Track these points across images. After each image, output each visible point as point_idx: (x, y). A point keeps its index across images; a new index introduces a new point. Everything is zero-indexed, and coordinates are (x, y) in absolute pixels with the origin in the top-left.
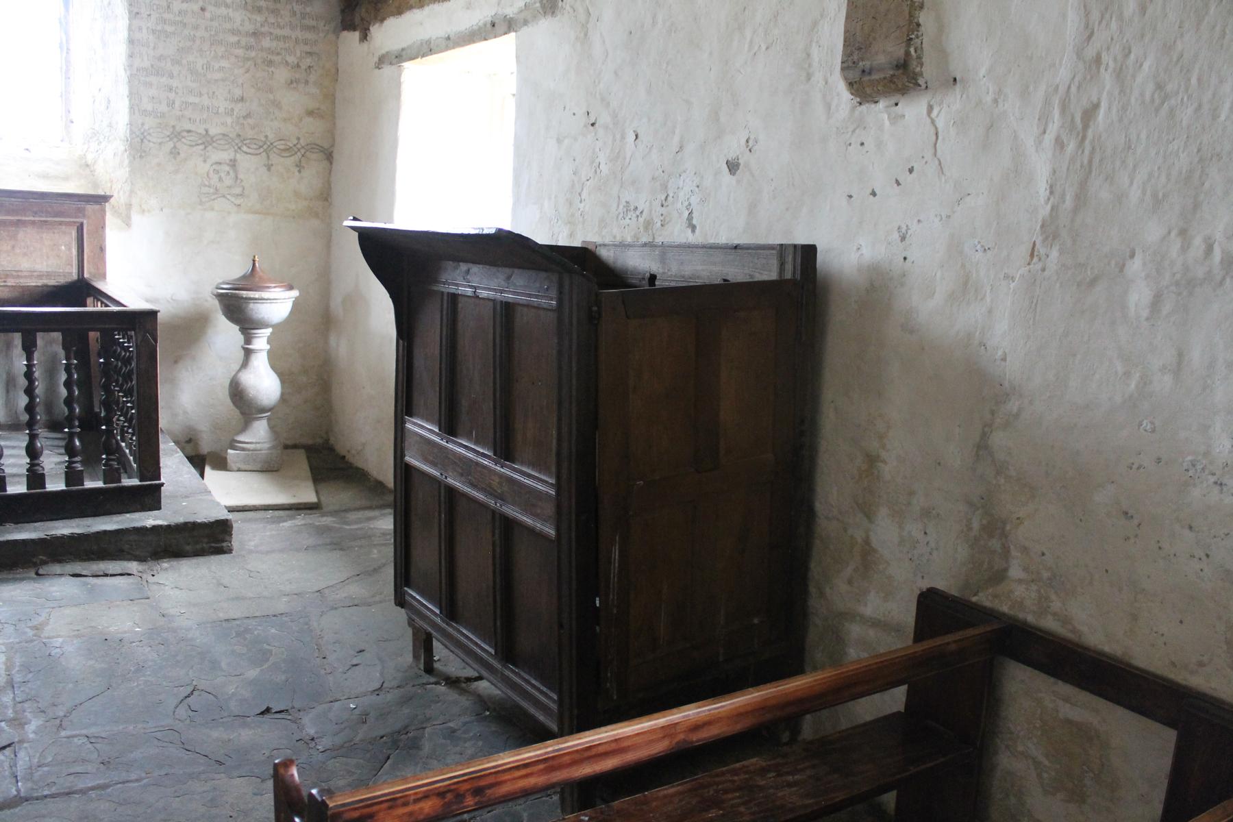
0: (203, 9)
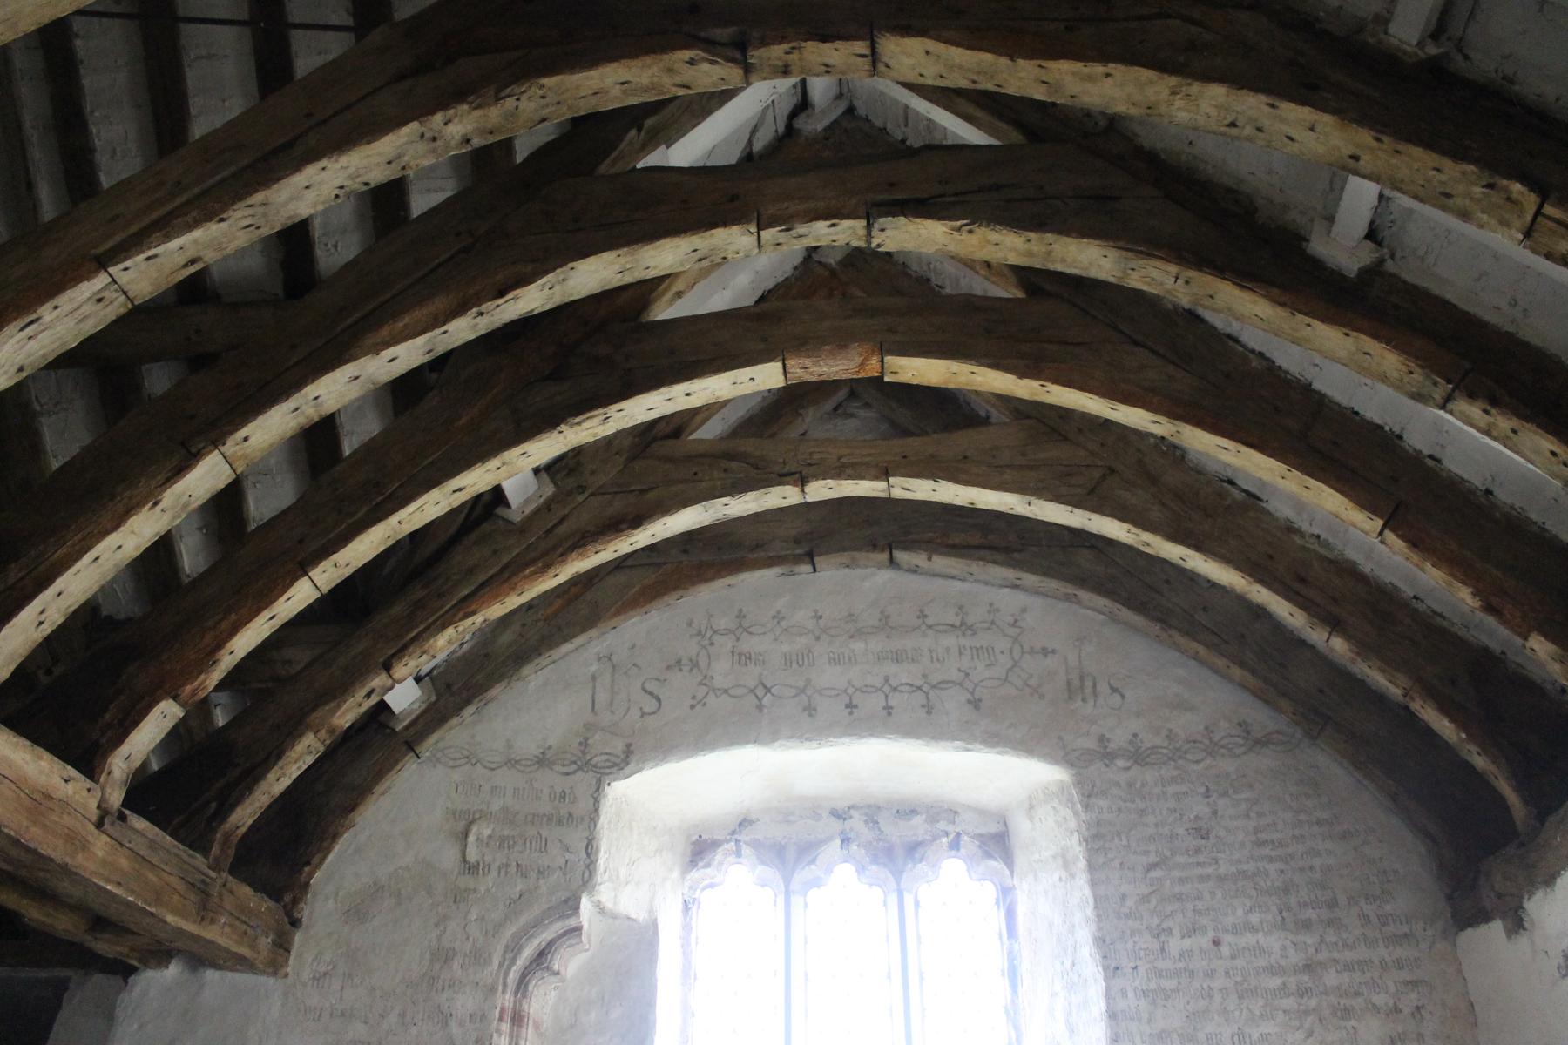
0: (1216, 943)
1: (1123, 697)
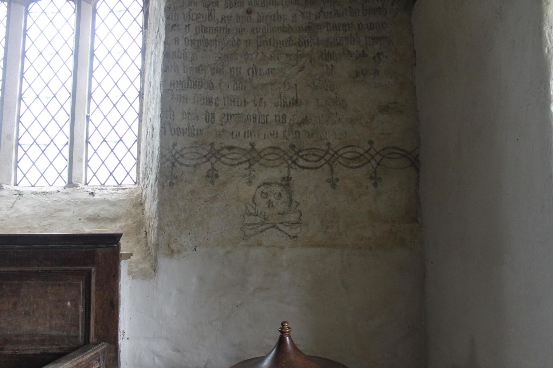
0: (249, 12)
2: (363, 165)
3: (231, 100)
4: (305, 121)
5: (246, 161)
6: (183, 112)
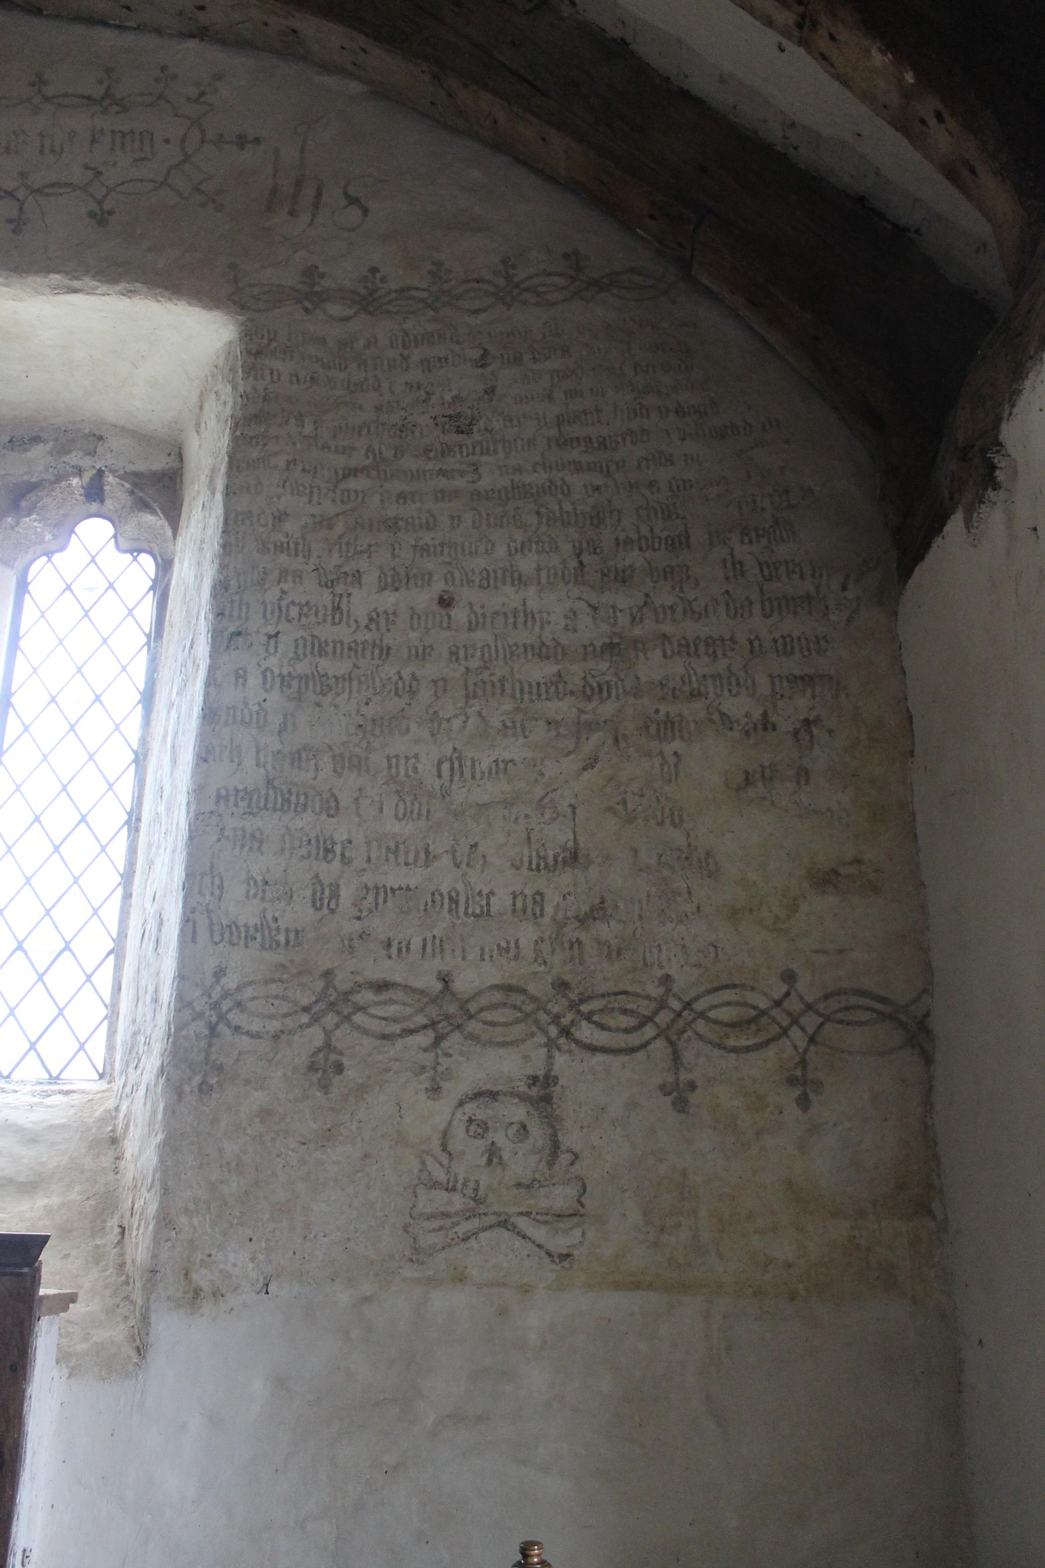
0: (445, 602)
1: (366, 211)
2: (767, 1043)
3: (388, 848)
4: (599, 911)
5: (425, 1027)
6: (250, 879)
